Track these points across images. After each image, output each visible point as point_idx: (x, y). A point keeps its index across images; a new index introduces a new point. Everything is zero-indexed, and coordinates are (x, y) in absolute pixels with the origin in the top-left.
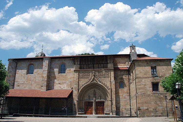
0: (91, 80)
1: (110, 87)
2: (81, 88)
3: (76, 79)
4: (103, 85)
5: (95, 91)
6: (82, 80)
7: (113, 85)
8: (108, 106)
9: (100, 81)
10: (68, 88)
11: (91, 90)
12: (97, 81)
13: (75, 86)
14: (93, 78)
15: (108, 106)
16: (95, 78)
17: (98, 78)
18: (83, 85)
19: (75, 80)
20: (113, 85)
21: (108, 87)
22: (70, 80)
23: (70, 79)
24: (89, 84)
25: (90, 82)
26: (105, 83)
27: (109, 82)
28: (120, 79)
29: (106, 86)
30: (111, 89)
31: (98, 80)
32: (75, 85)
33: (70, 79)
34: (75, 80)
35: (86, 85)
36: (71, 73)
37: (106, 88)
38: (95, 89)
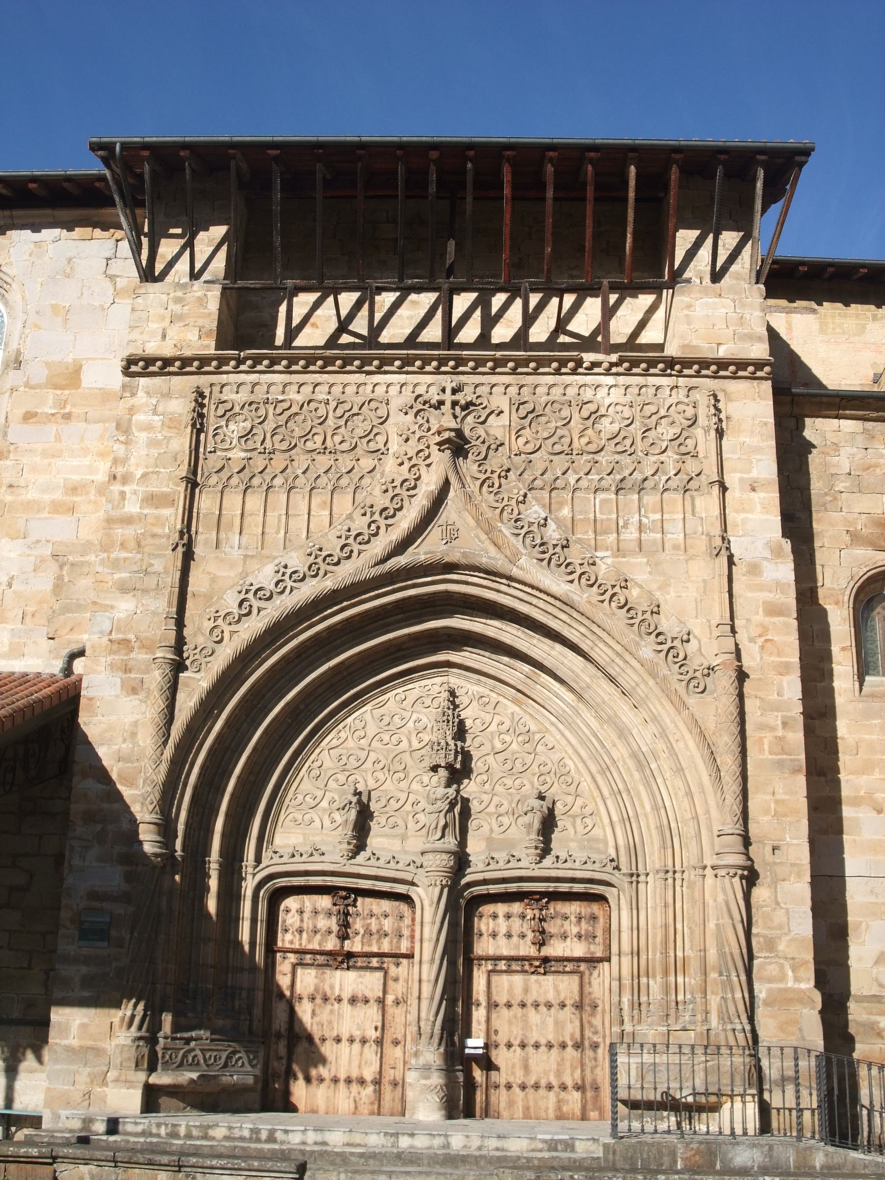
1: (708, 649)
3: (152, 500)
6: (254, 524)
7: (773, 610)
8: (679, 966)
9: (553, 533)
10: (16, 651)
13: (125, 606)
14: (430, 483)
15: (679, 966)
17: (514, 487)
19: (128, 520)
20: (773, 610)
22: (59, 530)
23: (57, 508)
26: (639, 570)
27: (707, 571)
28: (856, 538)
30: (742, 676)
32: (124, 589)
33: (57, 508)
34: (132, 507)
36: (77, 426)
38: (455, 679)
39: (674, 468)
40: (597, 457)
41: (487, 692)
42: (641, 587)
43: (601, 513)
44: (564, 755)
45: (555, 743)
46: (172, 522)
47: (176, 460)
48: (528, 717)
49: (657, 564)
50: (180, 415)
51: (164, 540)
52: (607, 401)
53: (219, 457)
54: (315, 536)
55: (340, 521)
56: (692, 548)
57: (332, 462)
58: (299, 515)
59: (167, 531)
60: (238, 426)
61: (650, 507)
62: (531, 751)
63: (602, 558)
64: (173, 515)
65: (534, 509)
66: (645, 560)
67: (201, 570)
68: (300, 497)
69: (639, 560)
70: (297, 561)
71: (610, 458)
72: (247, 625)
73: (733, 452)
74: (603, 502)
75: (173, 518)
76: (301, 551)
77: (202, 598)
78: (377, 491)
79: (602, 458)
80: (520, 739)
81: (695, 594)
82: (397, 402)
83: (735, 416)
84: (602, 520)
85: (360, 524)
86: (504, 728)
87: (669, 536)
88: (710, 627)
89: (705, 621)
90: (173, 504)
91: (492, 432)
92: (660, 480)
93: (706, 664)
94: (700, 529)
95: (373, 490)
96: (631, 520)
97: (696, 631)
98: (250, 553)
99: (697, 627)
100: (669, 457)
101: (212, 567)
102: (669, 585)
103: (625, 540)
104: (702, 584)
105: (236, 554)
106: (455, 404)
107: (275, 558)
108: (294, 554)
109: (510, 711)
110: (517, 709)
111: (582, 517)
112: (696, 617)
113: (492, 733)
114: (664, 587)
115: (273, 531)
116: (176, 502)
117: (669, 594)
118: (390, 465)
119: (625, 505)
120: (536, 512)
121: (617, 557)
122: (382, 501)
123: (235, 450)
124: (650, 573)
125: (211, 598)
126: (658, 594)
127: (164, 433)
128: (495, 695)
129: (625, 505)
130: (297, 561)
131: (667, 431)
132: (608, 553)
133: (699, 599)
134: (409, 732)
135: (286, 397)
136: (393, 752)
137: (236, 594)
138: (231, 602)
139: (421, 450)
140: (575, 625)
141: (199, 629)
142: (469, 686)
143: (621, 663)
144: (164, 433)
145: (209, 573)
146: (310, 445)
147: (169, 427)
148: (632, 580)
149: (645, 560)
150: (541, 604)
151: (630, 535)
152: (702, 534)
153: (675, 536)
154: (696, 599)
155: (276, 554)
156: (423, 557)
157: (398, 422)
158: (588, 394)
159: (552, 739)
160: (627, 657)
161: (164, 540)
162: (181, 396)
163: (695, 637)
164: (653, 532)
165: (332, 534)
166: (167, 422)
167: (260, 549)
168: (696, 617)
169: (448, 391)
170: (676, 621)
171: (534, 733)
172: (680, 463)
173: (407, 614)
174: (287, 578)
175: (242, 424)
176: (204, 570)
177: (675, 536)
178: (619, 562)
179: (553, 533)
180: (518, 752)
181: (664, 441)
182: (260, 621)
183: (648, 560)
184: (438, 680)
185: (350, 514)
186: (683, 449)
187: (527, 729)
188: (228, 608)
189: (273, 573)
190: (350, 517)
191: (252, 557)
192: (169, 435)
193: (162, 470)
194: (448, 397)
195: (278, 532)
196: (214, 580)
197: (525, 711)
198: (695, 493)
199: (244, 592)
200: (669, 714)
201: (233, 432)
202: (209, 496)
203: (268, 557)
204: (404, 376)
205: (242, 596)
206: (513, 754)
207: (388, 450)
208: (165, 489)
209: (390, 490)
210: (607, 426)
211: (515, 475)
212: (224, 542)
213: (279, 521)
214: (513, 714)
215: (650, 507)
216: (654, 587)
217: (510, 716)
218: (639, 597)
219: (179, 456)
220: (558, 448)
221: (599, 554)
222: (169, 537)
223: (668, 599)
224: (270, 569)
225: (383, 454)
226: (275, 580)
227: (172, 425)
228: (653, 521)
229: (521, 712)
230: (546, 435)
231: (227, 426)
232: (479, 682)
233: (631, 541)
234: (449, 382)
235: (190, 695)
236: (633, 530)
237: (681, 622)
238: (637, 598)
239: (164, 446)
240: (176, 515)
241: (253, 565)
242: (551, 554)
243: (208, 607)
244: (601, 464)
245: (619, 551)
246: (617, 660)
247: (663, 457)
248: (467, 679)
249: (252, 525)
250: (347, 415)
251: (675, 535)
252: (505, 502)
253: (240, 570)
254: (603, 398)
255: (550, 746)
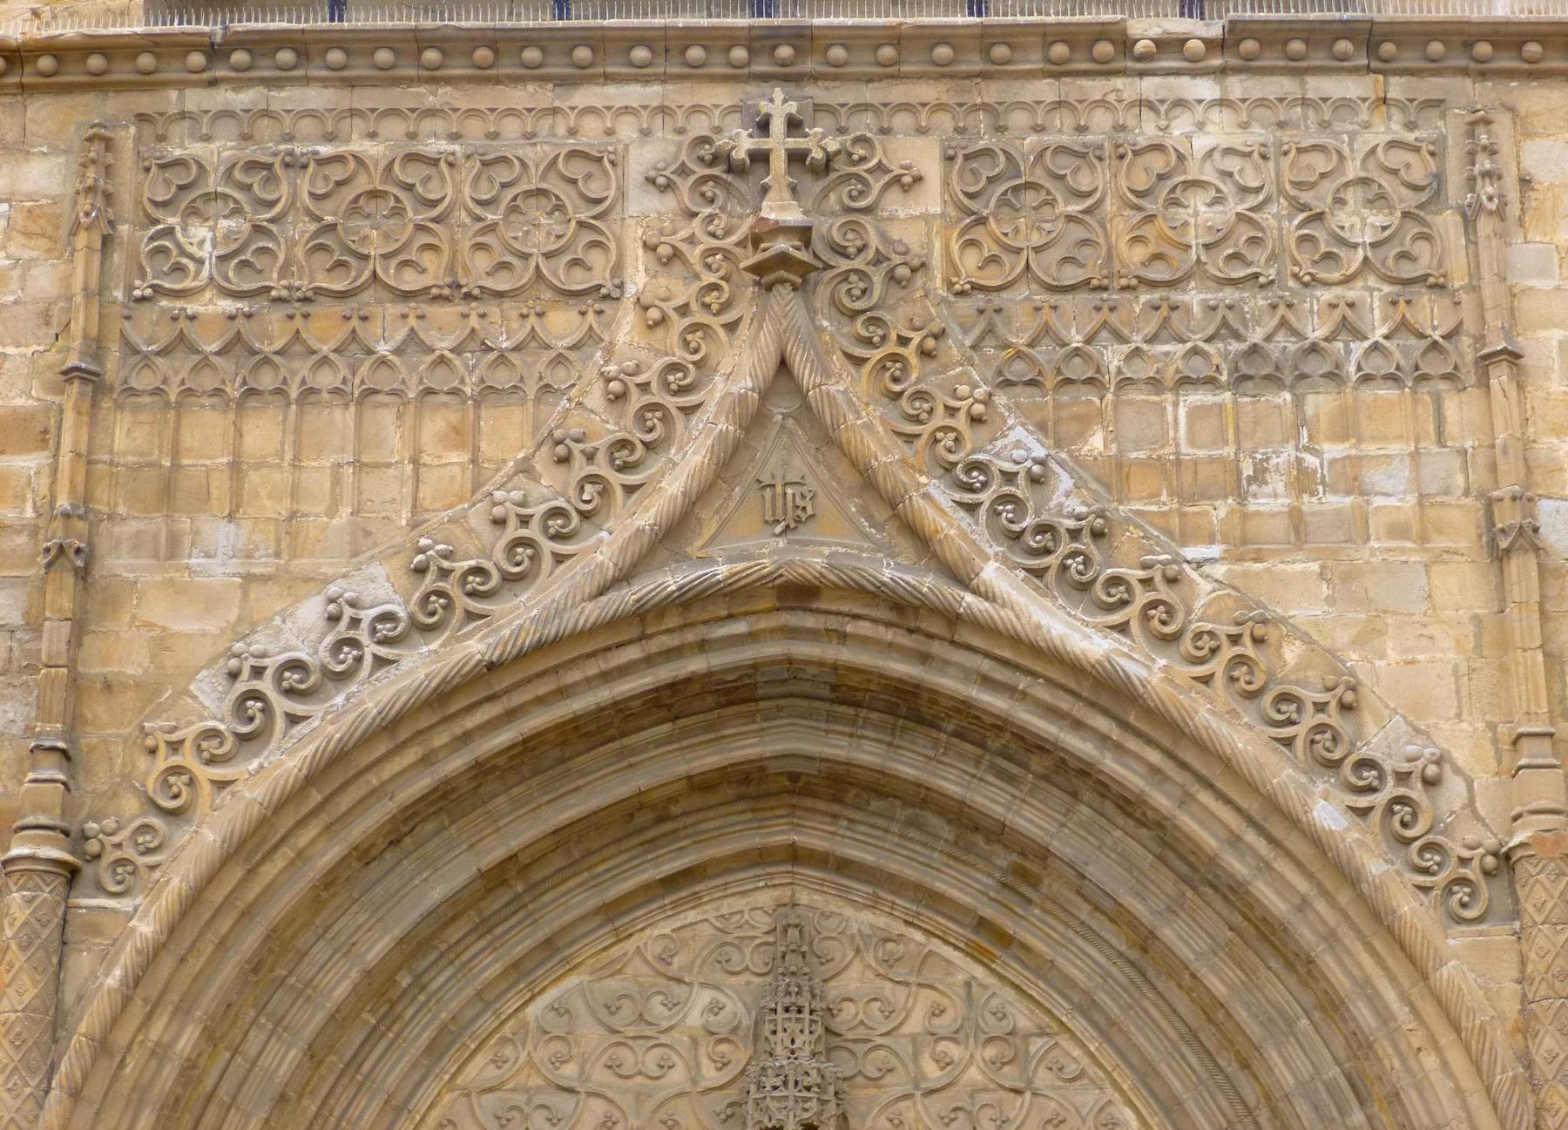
0: (655, 413)
2: (204, 837)
4: (1209, 713)
5: (795, 959)
11: (654, 931)
12: (936, 504)
14: (738, 370)
16: (845, 391)
17: (965, 378)
18: (300, 680)
21: (1399, 800)
24: (545, 653)
25: (603, 548)
26: (1301, 598)
29: (1324, 725)
31: (967, 478)
35: (421, 665)
37: (1327, 811)
39: (1384, 320)
40: (1177, 296)
41: (899, 928)
42: (1306, 639)
43: (1193, 443)
44: (1110, 1091)
45: (1086, 1061)
46: (44, 491)
47: (48, 324)
48: (1010, 994)
49: (1348, 577)
50: (55, 201)
51: (21, 540)
52: (1201, 143)
53: (164, 311)
54: (434, 519)
55: (498, 478)
56: (1440, 531)
57: (474, 322)
58: (388, 466)
59: (29, 513)
60: (213, 229)
61: (1323, 425)
62: (1020, 1085)
63: (1199, 565)
64: (46, 472)
65: (1013, 436)
66: (1314, 567)
67: (126, 618)
68: (388, 416)
69: (1298, 567)
70: (382, 589)
71: (1211, 297)
72: (254, 764)
73: (1543, 273)
74: (1196, 413)
75: (44, 481)
76: (398, 562)
77: (131, 694)
78: (595, 398)
79: (1194, 297)
80: (990, 1052)
81: (1452, 655)
82: (643, 157)
83: (1542, 176)
84: (1195, 463)
85: (550, 488)
86: (944, 1023)
87: (1378, 501)
88: (1495, 741)
89: (1481, 725)
90: (44, 441)
91: (896, 233)
92: (1348, 351)
93: (1491, 842)
94: (1460, 480)
95: (584, 393)
96: (1274, 461)
97: (1461, 756)
98: (257, 571)
99: (1463, 741)
100: (1371, 290)
101: (156, 610)
102: (1382, 633)
103: (1258, 514)
104: (1469, 629)
105: (219, 571)
106: (796, 158)
107: (328, 581)
108: (379, 570)
109: (960, 978)
110: (979, 972)
111: (1142, 455)
112: (1459, 716)
113: (914, 1038)
114: (1368, 636)
115: (319, 509)
116: (51, 436)
117: (1383, 656)
118: (626, 329)
119: (1256, 422)
120: (1018, 444)
121: (1240, 559)
122: (608, 427)
123: (208, 295)
124: (1330, 601)
125: (158, 692)
126: (1353, 657)
127: (12, 249)
128: (918, 936)
129: (1256, 422)
130: (382, 589)
131: (1360, 223)
132: (1215, 551)
133: (1464, 669)
134: (694, 1041)
135: (342, 149)
136: (649, 1096)
137: (221, 683)
138: (209, 702)
139: (714, 287)
140: (1133, 744)
141: (126, 777)
142: (848, 911)
143: (1261, 845)
144: (12, 249)
145: (150, 625)
146: (410, 281)
147: (27, 235)
148: (1284, 620)
149: (1314, 567)
150: (1042, 692)
151: (1271, 500)
152: (1467, 493)
153: (1393, 501)
154: (1456, 668)
155: (331, 571)
156: (722, 571)
157: (643, 212)
158: (1147, 129)
159: (1077, 1053)
160: (1277, 829)
161: (21, 540)
162: (55, 150)
163: (1458, 771)
164: (1335, 492)
165: (477, 518)
166: (20, 219)
167: (285, 557)
168: (1459, 716)
169: (778, 126)
170: (1404, 728)
171: (1027, 1037)
172: (1402, 304)
173: (681, 722)
174: (355, 641)
175: (224, 224)
176: (134, 617)
177: (1393, 501)
178: (1246, 574)
179: (1066, 500)
180: (985, 1090)
181: (1355, 246)
182: (290, 753)
183: (1323, 567)
184: (765, 898)
185: (526, 459)
186: (1408, 271)
187: (1006, 1026)
188: (203, 718)
189: (321, 623)
190: (525, 469)
191: (265, 579)
192: (27, 254)
193: (10, 350)
194: (778, 142)
195: (331, 512)
196: (162, 643)
197: (1002, 978)
198: (1443, 386)
199: (246, 673)
200: (1393, 979)
201: (201, 243)
202: (142, 417)
203: (307, 580)
204: (657, 88)
205: (241, 687)
206: (972, 1096)
207: (621, 286)
208: (20, 402)
209: (634, 393)
210: (1200, 213)
211: (961, 345)
212: (187, 540)
213: (336, 481)
214: (968, 985)
215: (1323, 425)
216: (1342, 637)
217: (962, 992)
218: (1302, 666)
219: (55, 311)
220: (1071, 275)
221: (1191, 552)
222: (34, 531)
223: (1381, 670)
224: (311, 611)
225: (607, 297)
226: (330, 639)
227: (32, 227)
228: (1333, 462)
229: (991, 980)
230: (1036, 239)
231: (184, 230)
232: (873, 904)
233: (1274, 515)
234: (779, 105)
235: (106, 960)
236: (1280, 487)
237: (1417, 731)
238: (1299, 667)
239: (14, 286)
240: (54, 470)
241: (267, 600)
242: (1063, 556)
243: (147, 719)
244: (1189, 311)
245: (1244, 546)
246: (1251, 837)
247: (1352, 294)
248: (844, 895)
249: (263, 492)
250: (509, 194)
251: (1392, 495)
252: (940, 419)
253: (233, 615)
254: (1189, 137)
255: (1071, 1070)
